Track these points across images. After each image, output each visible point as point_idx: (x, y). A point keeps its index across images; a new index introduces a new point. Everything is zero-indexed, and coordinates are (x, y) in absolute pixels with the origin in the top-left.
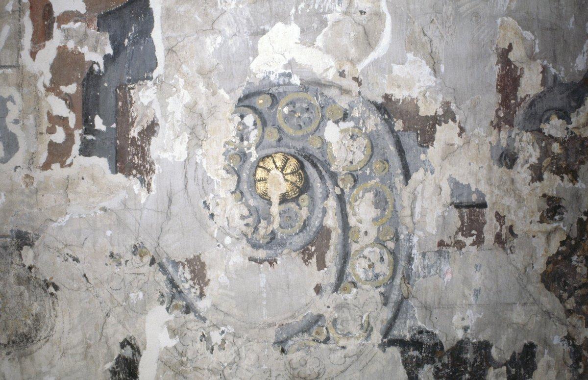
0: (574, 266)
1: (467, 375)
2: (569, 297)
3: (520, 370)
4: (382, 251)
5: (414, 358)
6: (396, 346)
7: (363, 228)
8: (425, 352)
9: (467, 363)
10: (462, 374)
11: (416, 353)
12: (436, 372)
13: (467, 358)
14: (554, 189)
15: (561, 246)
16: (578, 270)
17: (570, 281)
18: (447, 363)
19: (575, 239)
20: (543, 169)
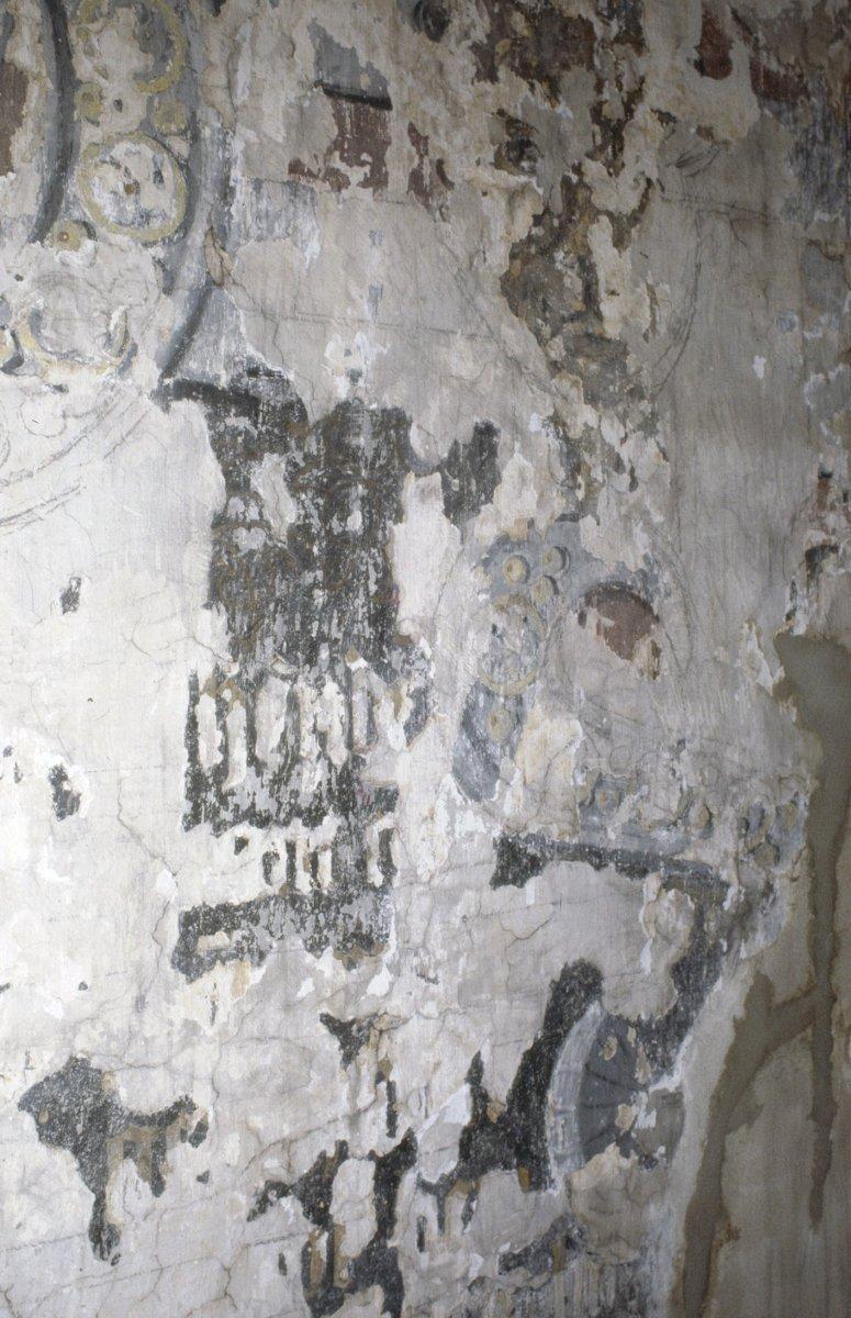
0: (559, 271)
1: (360, 487)
2: (553, 335)
3: (469, 484)
4: (159, 158)
5: (240, 434)
6: (195, 399)
7: (113, 89)
8: (264, 423)
9: (360, 458)
10: (349, 485)
11: (243, 423)
12: (290, 473)
13: (358, 448)
14: (519, 106)
15: (535, 225)
16: (567, 281)
17: (553, 301)
18: (315, 453)
19: (559, 217)
20: (497, 57)
